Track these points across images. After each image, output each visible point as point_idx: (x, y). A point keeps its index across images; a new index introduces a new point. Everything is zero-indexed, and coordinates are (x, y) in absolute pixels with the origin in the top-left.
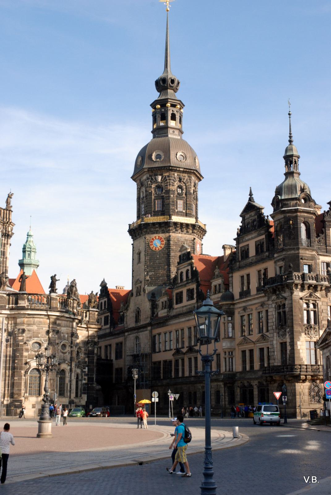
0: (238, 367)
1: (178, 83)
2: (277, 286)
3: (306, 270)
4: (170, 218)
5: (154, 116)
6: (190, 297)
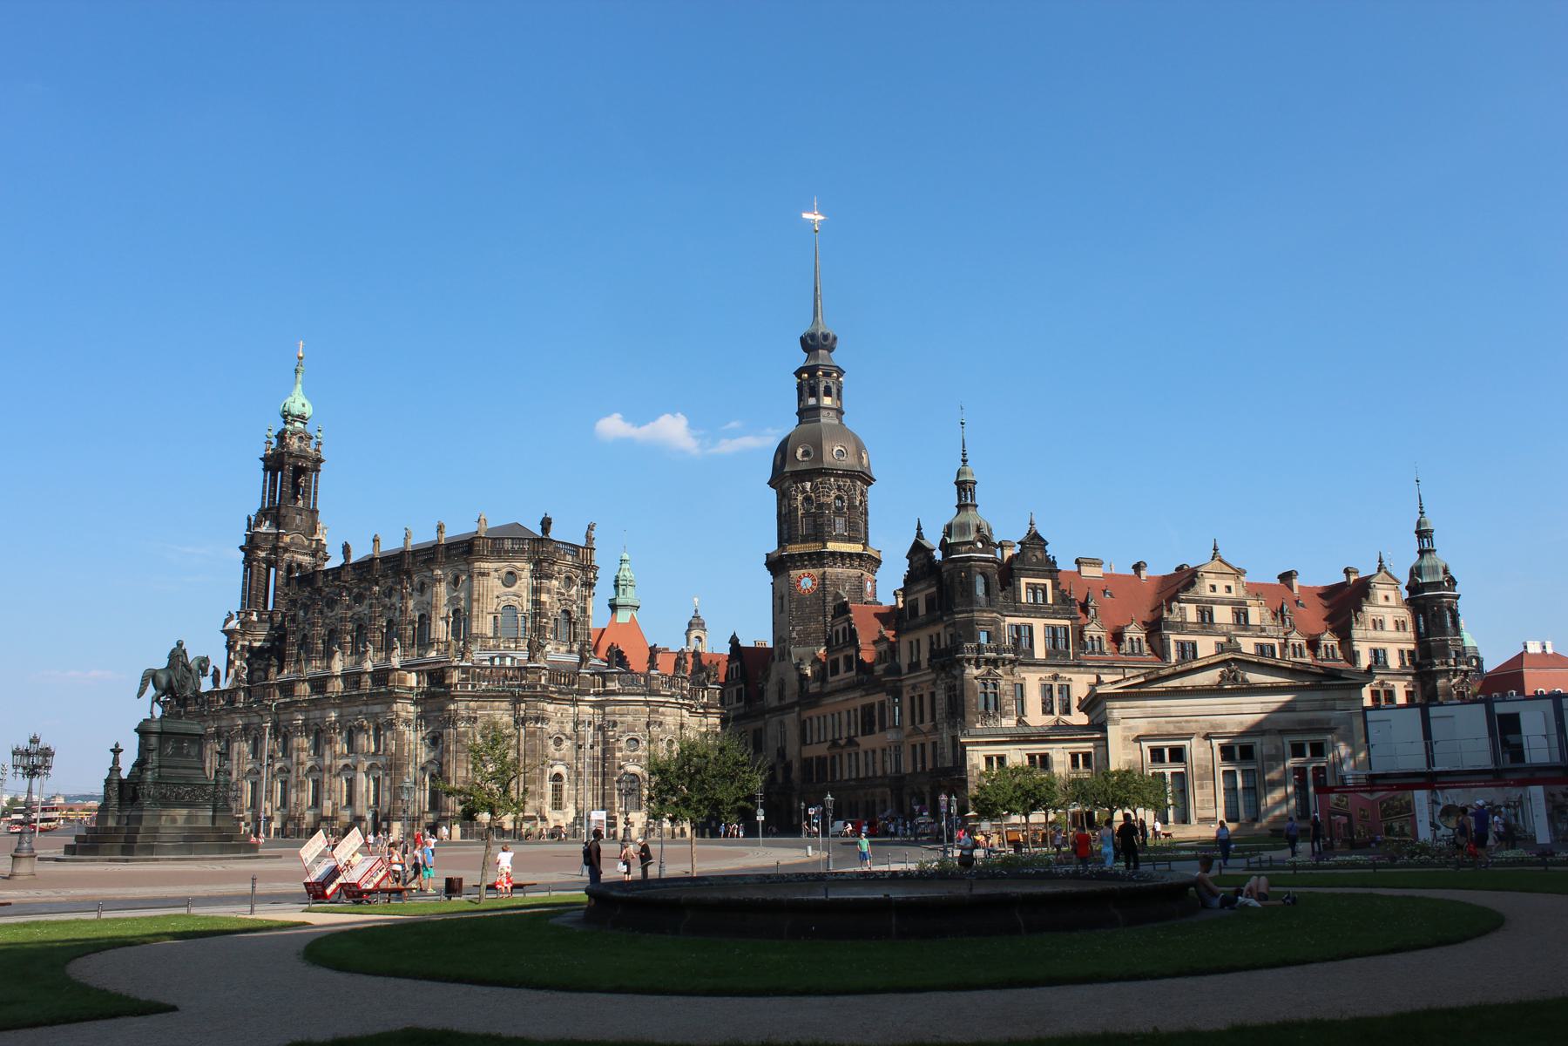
0: (907, 767)
1: (835, 339)
2: (947, 661)
3: (983, 638)
4: (825, 546)
5: (800, 388)
6: (849, 668)
